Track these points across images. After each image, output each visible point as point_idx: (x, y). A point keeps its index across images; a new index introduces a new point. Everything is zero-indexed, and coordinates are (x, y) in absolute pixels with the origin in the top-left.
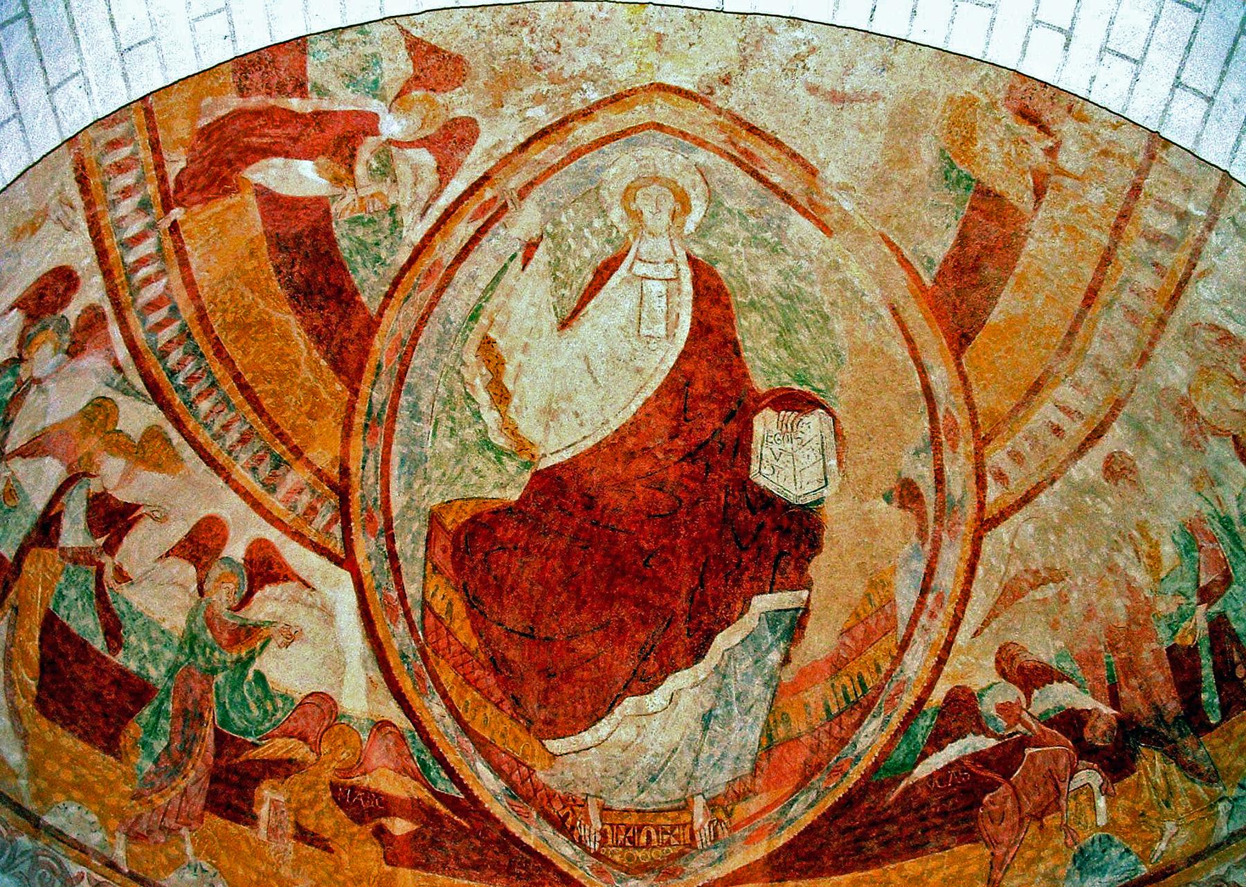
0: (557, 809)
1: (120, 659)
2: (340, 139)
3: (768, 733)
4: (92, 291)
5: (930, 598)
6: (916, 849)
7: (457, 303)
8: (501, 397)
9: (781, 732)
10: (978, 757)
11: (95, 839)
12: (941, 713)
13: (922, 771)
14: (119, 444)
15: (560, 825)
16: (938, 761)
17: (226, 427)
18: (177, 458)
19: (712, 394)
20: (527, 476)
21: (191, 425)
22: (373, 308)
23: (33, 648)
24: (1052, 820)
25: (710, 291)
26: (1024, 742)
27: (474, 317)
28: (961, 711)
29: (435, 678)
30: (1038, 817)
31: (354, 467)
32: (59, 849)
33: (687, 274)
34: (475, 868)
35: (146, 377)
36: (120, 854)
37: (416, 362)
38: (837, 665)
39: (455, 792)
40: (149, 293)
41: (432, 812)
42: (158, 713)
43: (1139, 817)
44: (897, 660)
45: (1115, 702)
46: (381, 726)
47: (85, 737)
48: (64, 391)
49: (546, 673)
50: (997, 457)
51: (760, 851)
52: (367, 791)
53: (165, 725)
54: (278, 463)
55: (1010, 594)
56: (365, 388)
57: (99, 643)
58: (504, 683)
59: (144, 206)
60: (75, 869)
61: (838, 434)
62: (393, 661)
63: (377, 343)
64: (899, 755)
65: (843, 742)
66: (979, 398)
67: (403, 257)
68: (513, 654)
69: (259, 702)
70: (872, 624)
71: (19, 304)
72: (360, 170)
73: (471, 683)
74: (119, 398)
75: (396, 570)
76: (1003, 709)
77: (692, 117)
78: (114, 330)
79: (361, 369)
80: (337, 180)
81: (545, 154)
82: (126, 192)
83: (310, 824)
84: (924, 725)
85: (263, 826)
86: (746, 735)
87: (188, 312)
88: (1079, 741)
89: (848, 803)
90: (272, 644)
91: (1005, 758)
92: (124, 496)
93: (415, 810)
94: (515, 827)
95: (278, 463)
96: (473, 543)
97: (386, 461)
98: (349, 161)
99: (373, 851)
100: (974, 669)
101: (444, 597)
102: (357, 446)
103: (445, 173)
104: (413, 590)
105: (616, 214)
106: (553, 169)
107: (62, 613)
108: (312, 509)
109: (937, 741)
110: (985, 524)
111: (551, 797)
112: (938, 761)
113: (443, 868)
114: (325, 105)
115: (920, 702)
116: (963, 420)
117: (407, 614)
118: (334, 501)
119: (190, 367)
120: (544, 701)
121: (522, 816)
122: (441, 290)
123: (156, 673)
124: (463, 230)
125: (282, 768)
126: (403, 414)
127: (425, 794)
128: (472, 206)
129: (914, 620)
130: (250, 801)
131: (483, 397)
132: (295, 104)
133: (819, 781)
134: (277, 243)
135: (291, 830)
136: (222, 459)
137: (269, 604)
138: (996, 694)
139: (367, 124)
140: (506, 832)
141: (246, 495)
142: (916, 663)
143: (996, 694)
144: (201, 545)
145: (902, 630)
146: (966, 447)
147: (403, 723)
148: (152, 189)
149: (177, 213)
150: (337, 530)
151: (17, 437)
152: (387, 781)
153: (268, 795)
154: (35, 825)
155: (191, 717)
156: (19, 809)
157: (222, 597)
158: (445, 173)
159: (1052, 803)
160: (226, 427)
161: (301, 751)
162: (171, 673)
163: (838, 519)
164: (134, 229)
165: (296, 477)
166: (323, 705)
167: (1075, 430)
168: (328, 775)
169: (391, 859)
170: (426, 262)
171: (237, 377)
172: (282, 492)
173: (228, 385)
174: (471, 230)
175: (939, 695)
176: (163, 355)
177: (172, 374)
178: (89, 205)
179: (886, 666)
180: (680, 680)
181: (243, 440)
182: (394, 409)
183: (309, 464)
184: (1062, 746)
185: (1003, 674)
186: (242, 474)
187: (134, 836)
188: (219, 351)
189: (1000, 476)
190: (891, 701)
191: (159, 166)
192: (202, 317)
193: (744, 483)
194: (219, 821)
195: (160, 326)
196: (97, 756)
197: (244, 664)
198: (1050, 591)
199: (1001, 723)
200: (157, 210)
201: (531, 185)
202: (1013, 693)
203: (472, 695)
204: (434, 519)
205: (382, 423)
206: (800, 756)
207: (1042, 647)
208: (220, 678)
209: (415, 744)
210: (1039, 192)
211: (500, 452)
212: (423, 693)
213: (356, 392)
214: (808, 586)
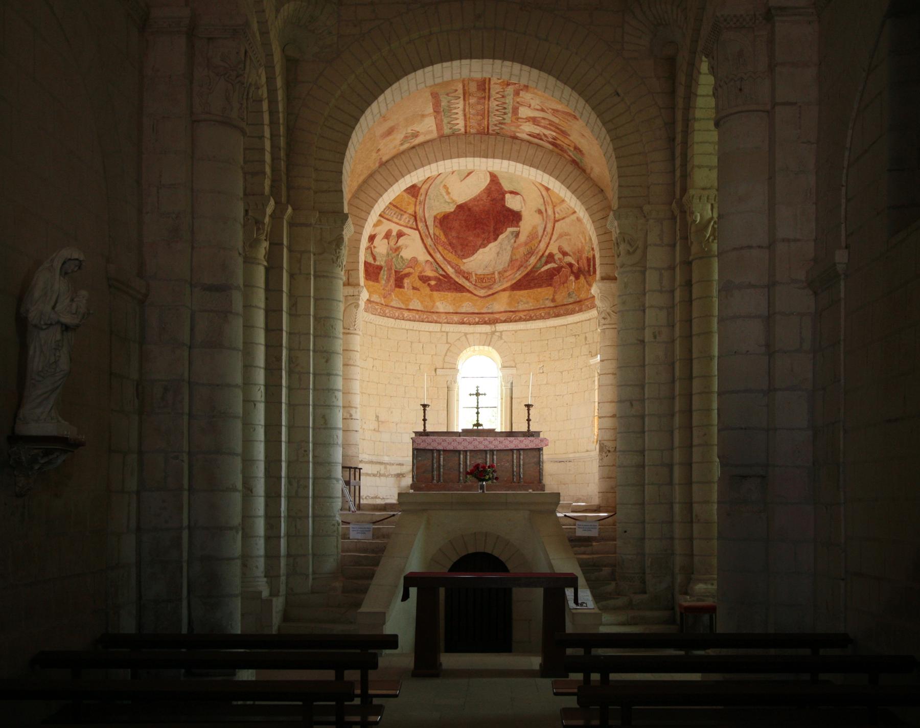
0: (466, 275)
3: (511, 258)
6: (540, 286)
8: (448, 193)
9: (514, 258)
10: (554, 268)
11: (378, 300)
13: (543, 269)
15: (467, 279)
16: (546, 268)
26: (562, 267)
28: (551, 258)
34: (449, 290)
38: (526, 244)
41: (439, 279)
46: (427, 261)
49: (462, 245)
50: (557, 209)
51: (509, 284)
55: (561, 236)
57: (372, 262)
58: (453, 248)
64: (538, 265)
70: (533, 236)
76: (559, 259)
84: (544, 259)
86: (506, 257)
89: (527, 274)
91: (558, 270)
93: (436, 278)
94: (457, 280)
96: (444, 221)
99: (428, 289)
100: (553, 249)
101: (439, 232)
102: (418, 207)
104: (431, 232)
109: (547, 263)
110: (556, 221)
112: (546, 268)
113: (443, 290)
120: (462, 251)
123: (383, 264)
125: (408, 275)
130: (402, 283)
131: (444, 194)
133: (522, 269)
137: (402, 241)
138: (558, 256)
142: (542, 245)
143: (558, 256)
144: (388, 236)
146: (551, 206)
147: (431, 260)
152: (429, 273)
153: (406, 281)
155: (390, 269)
157: (392, 243)
161: (411, 270)
163: (525, 214)
165: (406, 216)
166: (414, 260)
169: (432, 290)
175: (547, 253)
180: (492, 245)
184: (569, 270)
186: (395, 220)
187: (385, 297)
193: (504, 206)
196: (376, 284)
202: (560, 256)
203: (446, 252)
204: (435, 217)
205: (423, 203)
206: (518, 263)
207: (567, 249)
209: (434, 264)
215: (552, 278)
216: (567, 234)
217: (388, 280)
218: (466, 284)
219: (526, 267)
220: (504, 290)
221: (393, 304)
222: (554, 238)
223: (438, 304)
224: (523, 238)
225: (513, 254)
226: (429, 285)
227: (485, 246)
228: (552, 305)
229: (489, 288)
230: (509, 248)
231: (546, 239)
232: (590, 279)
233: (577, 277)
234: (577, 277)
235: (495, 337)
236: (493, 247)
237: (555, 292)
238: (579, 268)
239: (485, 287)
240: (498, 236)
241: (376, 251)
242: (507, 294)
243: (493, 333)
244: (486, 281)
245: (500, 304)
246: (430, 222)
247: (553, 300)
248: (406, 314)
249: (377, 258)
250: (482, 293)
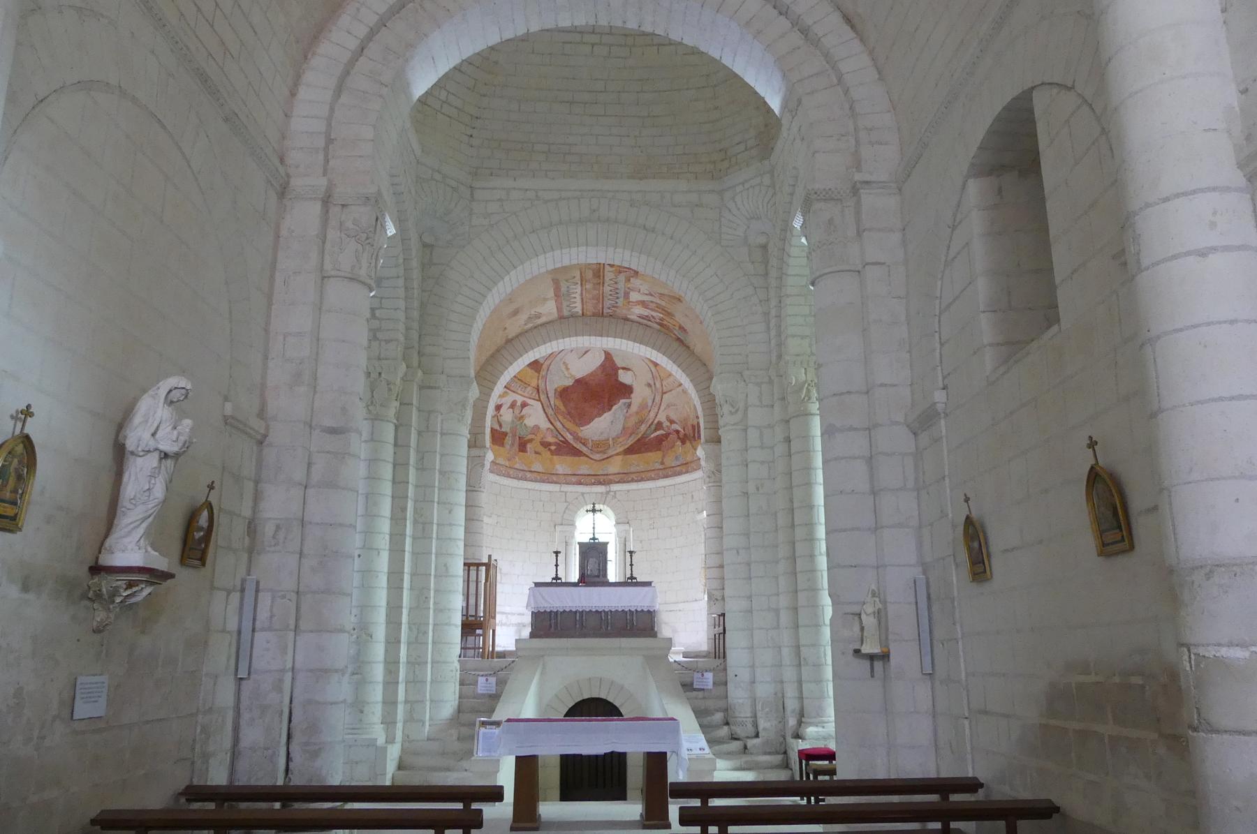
15: (584, 444)
34: (567, 454)
38: (637, 413)
55: (668, 406)
70: (643, 406)
84: (653, 427)
86: (619, 427)
91: (667, 435)
93: (556, 444)
96: (564, 393)
100: (662, 417)
109: (656, 430)
110: (664, 393)
125: (531, 441)
137: (525, 411)
138: (666, 424)
142: (652, 414)
143: (666, 424)
144: (513, 406)
152: (550, 439)
153: (529, 446)
157: (517, 411)
166: (537, 427)
207: (673, 417)
217: (513, 445)
218: (584, 449)
220: (617, 454)
221: (517, 466)
222: (662, 408)
223: (558, 467)
224: (634, 408)
227: (600, 415)
233: (683, 443)
234: (683, 443)
235: (610, 497)
236: (607, 416)
241: (501, 419)
242: (620, 458)
243: (608, 493)
244: (601, 446)
245: (615, 466)
246: (551, 394)
247: (662, 463)
248: (528, 475)
250: (597, 457)
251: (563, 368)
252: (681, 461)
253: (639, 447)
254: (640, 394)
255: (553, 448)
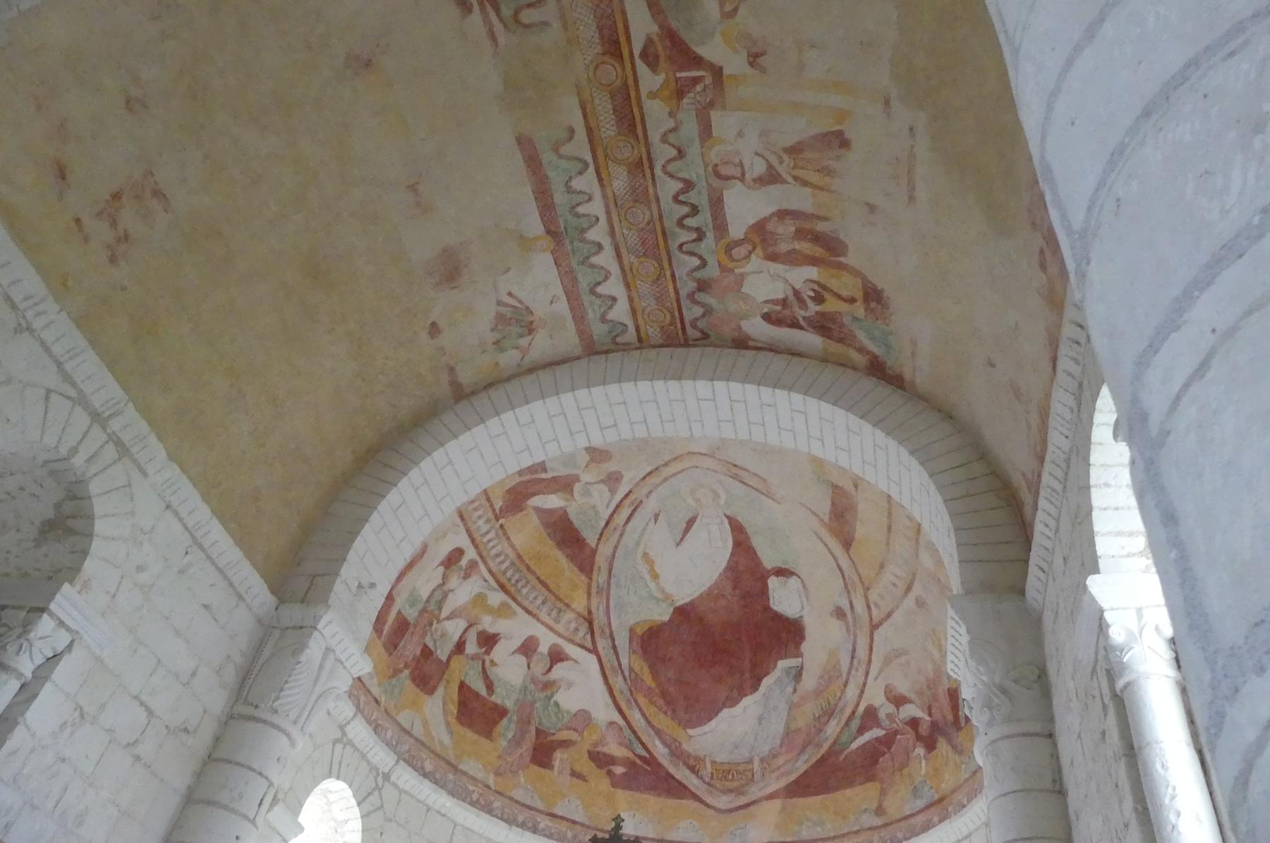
0: (692, 762)
1: (493, 698)
2: (565, 485)
4: (471, 554)
5: (855, 661)
6: (850, 784)
7: (628, 540)
8: (655, 576)
9: (793, 726)
10: (877, 739)
11: (480, 776)
12: (863, 718)
13: (854, 746)
14: (490, 611)
15: (693, 769)
17: (535, 598)
18: (515, 613)
19: (748, 572)
20: (671, 610)
21: (519, 598)
22: (593, 545)
23: (455, 696)
24: (905, 771)
25: (737, 528)
26: (896, 733)
27: (638, 544)
28: (871, 716)
29: (636, 701)
30: (901, 770)
31: (594, 610)
32: (464, 779)
33: (726, 522)
35: (498, 582)
36: (491, 782)
37: (616, 564)
38: (818, 693)
39: (644, 753)
40: (494, 552)
41: (634, 763)
42: (510, 721)
43: (936, 770)
44: (843, 692)
45: (930, 715)
46: (612, 723)
47: (479, 733)
48: (462, 593)
50: (873, 596)
51: (782, 783)
52: (605, 754)
53: (513, 726)
54: (560, 611)
55: (887, 661)
56: (595, 576)
57: (483, 692)
58: (668, 703)
59: (488, 521)
60: (471, 788)
61: (804, 586)
62: (617, 694)
63: (597, 558)
64: (844, 738)
65: (821, 730)
66: (860, 571)
67: (603, 524)
68: (671, 689)
69: (557, 716)
70: (831, 675)
71: (442, 564)
72: (576, 495)
73: (653, 703)
74: (487, 592)
75: (616, 653)
76: (889, 716)
77: (708, 462)
78: (482, 567)
79: (592, 570)
80: (567, 500)
81: (653, 480)
82: (479, 517)
83: (577, 768)
84: (855, 724)
85: (556, 768)
86: (776, 727)
87: (512, 555)
88: (917, 732)
89: (823, 760)
90: (561, 690)
91: (888, 741)
92: (492, 630)
94: (672, 770)
95: (560, 611)
96: (650, 640)
97: (608, 606)
98: (571, 492)
99: (607, 781)
100: (875, 697)
103: (613, 492)
104: (625, 662)
105: (690, 501)
106: (658, 486)
107: (467, 682)
108: (577, 629)
109: (861, 731)
110: (874, 627)
111: (689, 756)
113: (638, 789)
114: (555, 474)
115: (854, 712)
116: (856, 579)
117: (622, 673)
118: (587, 625)
119: (517, 576)
121: (675, 765)
122: (621, 535)
123: (509, 704)
124: (625, 512)
125: (565, 744)
126: (613, 586)
127: (631, 755)
128: (627, 502)
129: (849, 673)
131: (647, 577)
132: (543, 476)
133: (810, 749)
134: (547, 525)
135: (568, 771)
136: (535, 611)
137: (559, 671)
138: (885, 709)
139: (576, 479)
140: (668, 773)
141: (548, 626)
142: (852, 692)
143: (885, 709)
144: (528, 648)
145: (844, 676)
146: (860, 591)
147: (621, 722)
148: (490, 514)
149: (502, 521)
150: (588, 637)
151: (445, 612)
152: (614, 748)
153: (559, 756)
154: (455, 769)
155: (525, 722)
156: (449, 763)
157: (538, 669)
158: (613, 492)
159: (904, 765)
160: (535, 598)
161: (573, 736)
162: (515, 703)
164: (485, 528)
165: (569, 616)
167: (902, 586)
168: (586, 747)
169: (614, 785)
170: (612, 525)
171: (538, 578)
172: (563, 622)
173: (534, 582)
174: (630, 511)
175: (861, 709)
176: (505, 573)
177: (509, 580)
178: (465, 525)
179: (839, 694)
180: (747, 701)
181: (543, 603)
182: (609, 584)
183: (573, 610)
184: (911, 735)
185: (888, 699)
186: (544, 616)
188: (528, 568)
189: (876, 605)
190: (842, 710)
191: (492, 506)
192: (519, 556)
193: (767, 608)
194: (536, 768)
195: (502, 562)
196: (484, 742)
197: (549, 698)
198: (903, 659)
199: (888, 723)
200: (493, 521)
201: (650, 492)
202: (891, 708)
204: (632, 630)
205: (605, 591)
207: (903, 687)
208: (538, 705)
209: (627, 732)
210: (856, 486)
211: (658, 600)
212: (630, 709)
213: (591, 579)
214: (799, 655)
215: (877, 762)
216: (899, 653)
217: (517, 742)
219: (819, 745)
221: (518, 794)
224: (809, 681)
225: (790, 717)
226: (609, 773)
227: (732, 702)
228: (878, 821)
229: (739, 792)
230: (783, 707)
231: (858, 677)
232: (961, 738)
233: (930, 745)
234: (930, 745)
236: (750, 704)
237: (883, 792)
238: (934, 726)
239: (731, 791)
240: (759, 680)
242: (777, 803)
244: (732, 777)
248: (544, 822)
249: (498, 690)
250: (723, 802)
251: (643, 569)
252: (929, 795)
253: (823, 777)
254: (823, 641)
255: (619, 770)
